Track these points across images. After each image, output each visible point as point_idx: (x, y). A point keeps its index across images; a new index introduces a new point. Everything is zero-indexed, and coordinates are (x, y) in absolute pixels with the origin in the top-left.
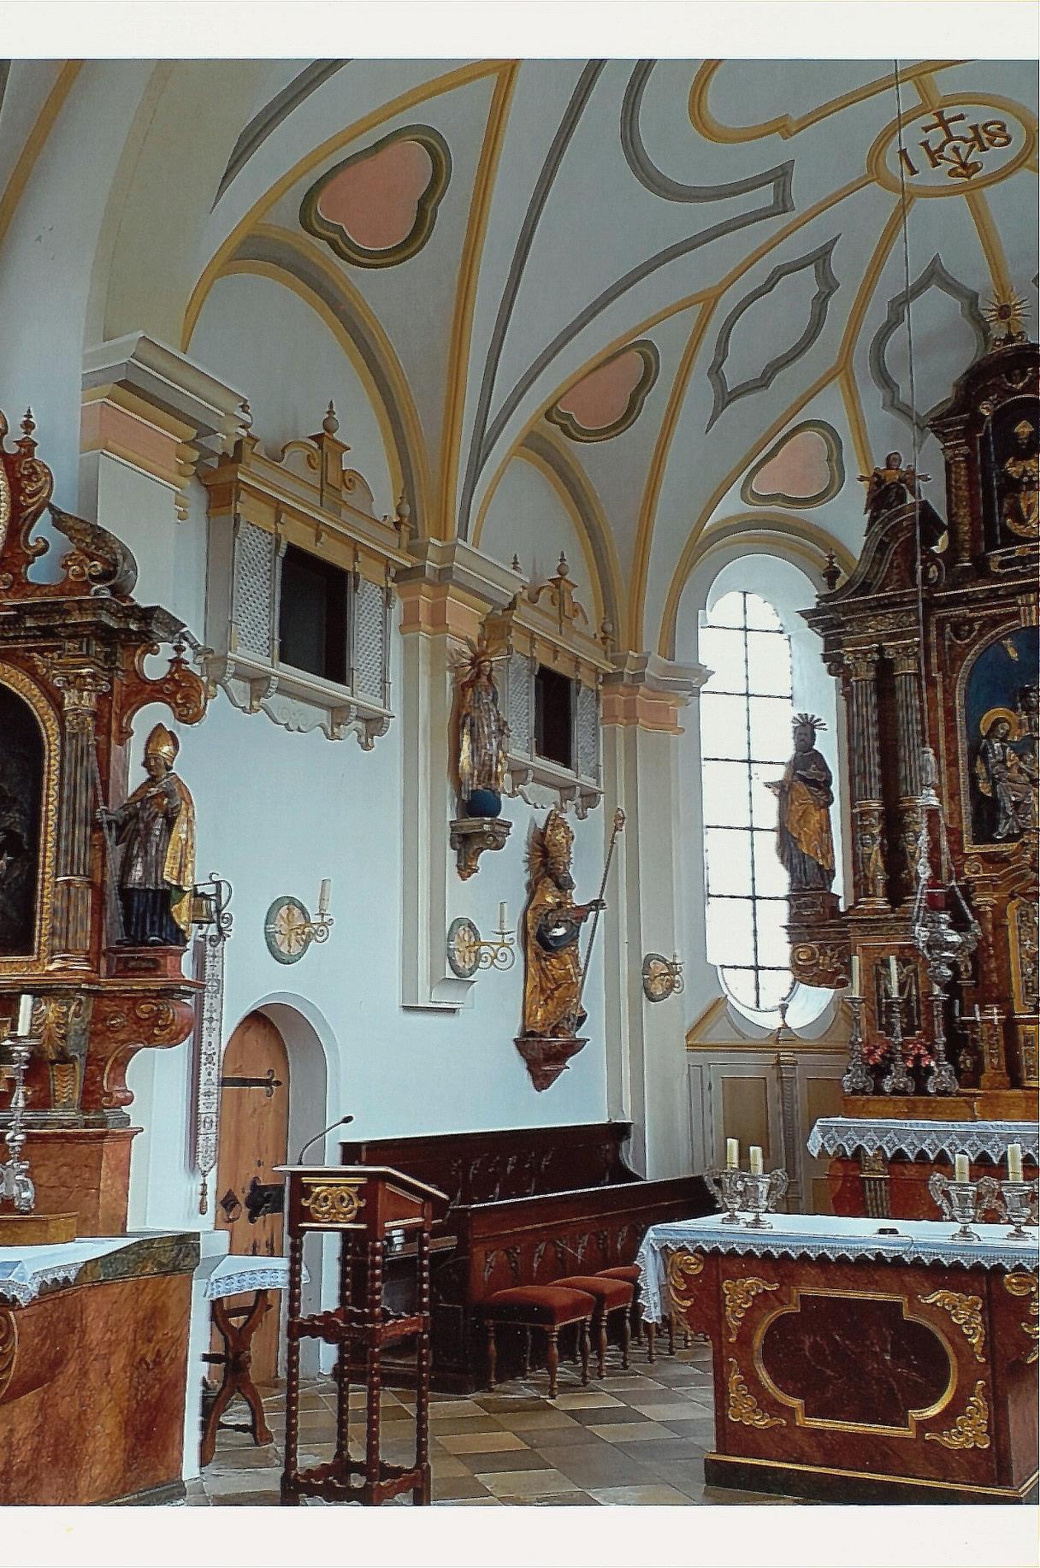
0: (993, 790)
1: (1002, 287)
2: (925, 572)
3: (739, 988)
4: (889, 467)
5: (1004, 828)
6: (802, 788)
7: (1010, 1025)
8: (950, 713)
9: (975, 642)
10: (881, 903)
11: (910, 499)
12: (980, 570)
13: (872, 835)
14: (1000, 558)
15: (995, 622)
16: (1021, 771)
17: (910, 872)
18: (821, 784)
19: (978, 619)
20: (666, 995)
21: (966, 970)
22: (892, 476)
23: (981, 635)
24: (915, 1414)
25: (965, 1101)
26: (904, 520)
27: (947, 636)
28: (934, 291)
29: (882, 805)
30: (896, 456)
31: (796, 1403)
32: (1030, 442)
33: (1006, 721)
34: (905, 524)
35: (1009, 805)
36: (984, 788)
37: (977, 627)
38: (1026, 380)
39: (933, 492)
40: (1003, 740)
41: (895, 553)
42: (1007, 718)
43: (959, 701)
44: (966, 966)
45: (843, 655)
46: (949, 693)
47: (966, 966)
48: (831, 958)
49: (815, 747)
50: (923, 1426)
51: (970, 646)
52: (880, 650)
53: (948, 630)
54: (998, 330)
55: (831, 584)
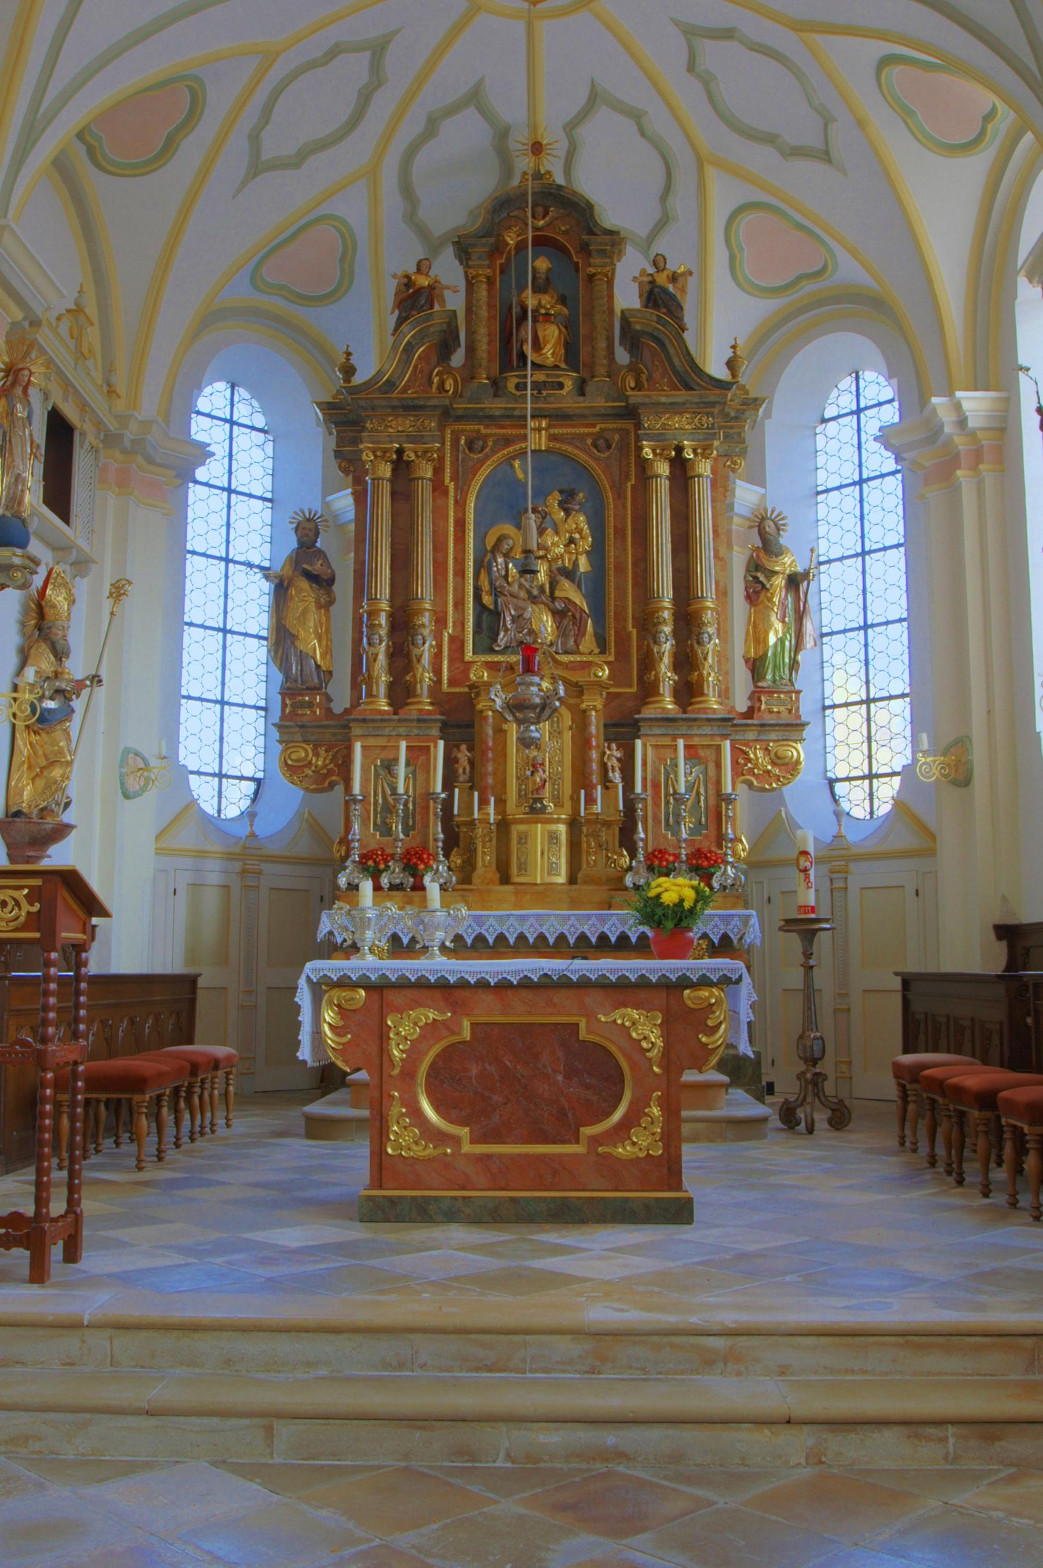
0: (496, 603)
1: (533, 127)
2: (442, 384)
3: (203, 791)
4: (419, 270)
5: (502, 639)
6: (304, 584)
7: (504, 825)
8: (460, 524)
9: (487, 457)
10: (383, 705)
11: (437, 307)
12: (497, 386)
13: (380, 637)
14: (516, 380)
15: (508, 441)
16: (521, 586)
17: (414, 676)
18: (324, 582)
19: (491, 435)
20: (143, 790)
21: (464, 772)
22: (423, 281)
23: (494, 452)
24: (587, 1131)
25: (463, 896)
26: (432, 325)
27: (461, 448)
28: (471, 114)
29: (391, 607)
30: (427, 263)
31: (464, 1132)
32: (547, 279)
33: (510, 538)
34: (432, 330)
35: (508, 619)
36: (487, 600)
37: (490, 444)
38: (547, 219)
39: (455, 301)
40: (506, 556)
41: (419, 358)
42: (513, 535)
43: (470, 516)
44: (464, 769)
45: (361, 451)
46: (461, 504)
47: (464, 769)
48: (325, 759)
49: (318, 545)
50: (595, 1141)
51: (482, 462)
52: (400, 452)
53: (462, 442)
54: (524, 163)
55: (347, 380)
